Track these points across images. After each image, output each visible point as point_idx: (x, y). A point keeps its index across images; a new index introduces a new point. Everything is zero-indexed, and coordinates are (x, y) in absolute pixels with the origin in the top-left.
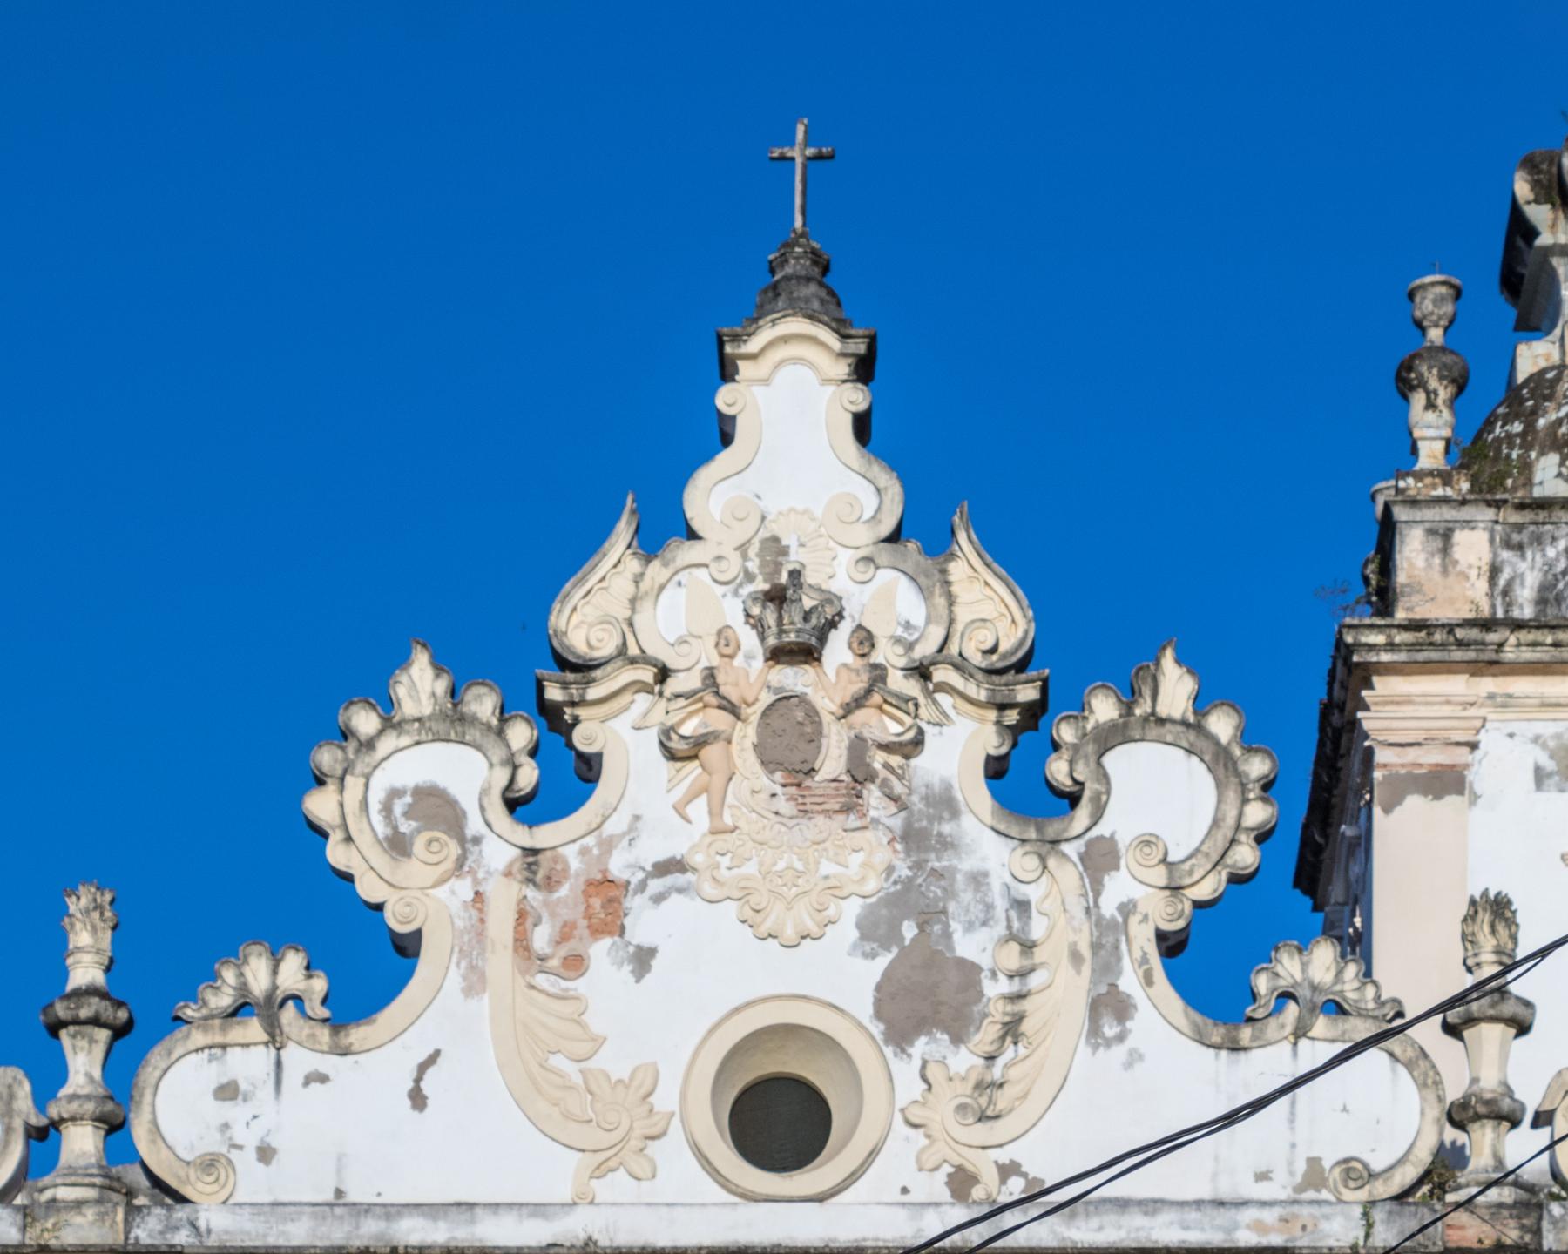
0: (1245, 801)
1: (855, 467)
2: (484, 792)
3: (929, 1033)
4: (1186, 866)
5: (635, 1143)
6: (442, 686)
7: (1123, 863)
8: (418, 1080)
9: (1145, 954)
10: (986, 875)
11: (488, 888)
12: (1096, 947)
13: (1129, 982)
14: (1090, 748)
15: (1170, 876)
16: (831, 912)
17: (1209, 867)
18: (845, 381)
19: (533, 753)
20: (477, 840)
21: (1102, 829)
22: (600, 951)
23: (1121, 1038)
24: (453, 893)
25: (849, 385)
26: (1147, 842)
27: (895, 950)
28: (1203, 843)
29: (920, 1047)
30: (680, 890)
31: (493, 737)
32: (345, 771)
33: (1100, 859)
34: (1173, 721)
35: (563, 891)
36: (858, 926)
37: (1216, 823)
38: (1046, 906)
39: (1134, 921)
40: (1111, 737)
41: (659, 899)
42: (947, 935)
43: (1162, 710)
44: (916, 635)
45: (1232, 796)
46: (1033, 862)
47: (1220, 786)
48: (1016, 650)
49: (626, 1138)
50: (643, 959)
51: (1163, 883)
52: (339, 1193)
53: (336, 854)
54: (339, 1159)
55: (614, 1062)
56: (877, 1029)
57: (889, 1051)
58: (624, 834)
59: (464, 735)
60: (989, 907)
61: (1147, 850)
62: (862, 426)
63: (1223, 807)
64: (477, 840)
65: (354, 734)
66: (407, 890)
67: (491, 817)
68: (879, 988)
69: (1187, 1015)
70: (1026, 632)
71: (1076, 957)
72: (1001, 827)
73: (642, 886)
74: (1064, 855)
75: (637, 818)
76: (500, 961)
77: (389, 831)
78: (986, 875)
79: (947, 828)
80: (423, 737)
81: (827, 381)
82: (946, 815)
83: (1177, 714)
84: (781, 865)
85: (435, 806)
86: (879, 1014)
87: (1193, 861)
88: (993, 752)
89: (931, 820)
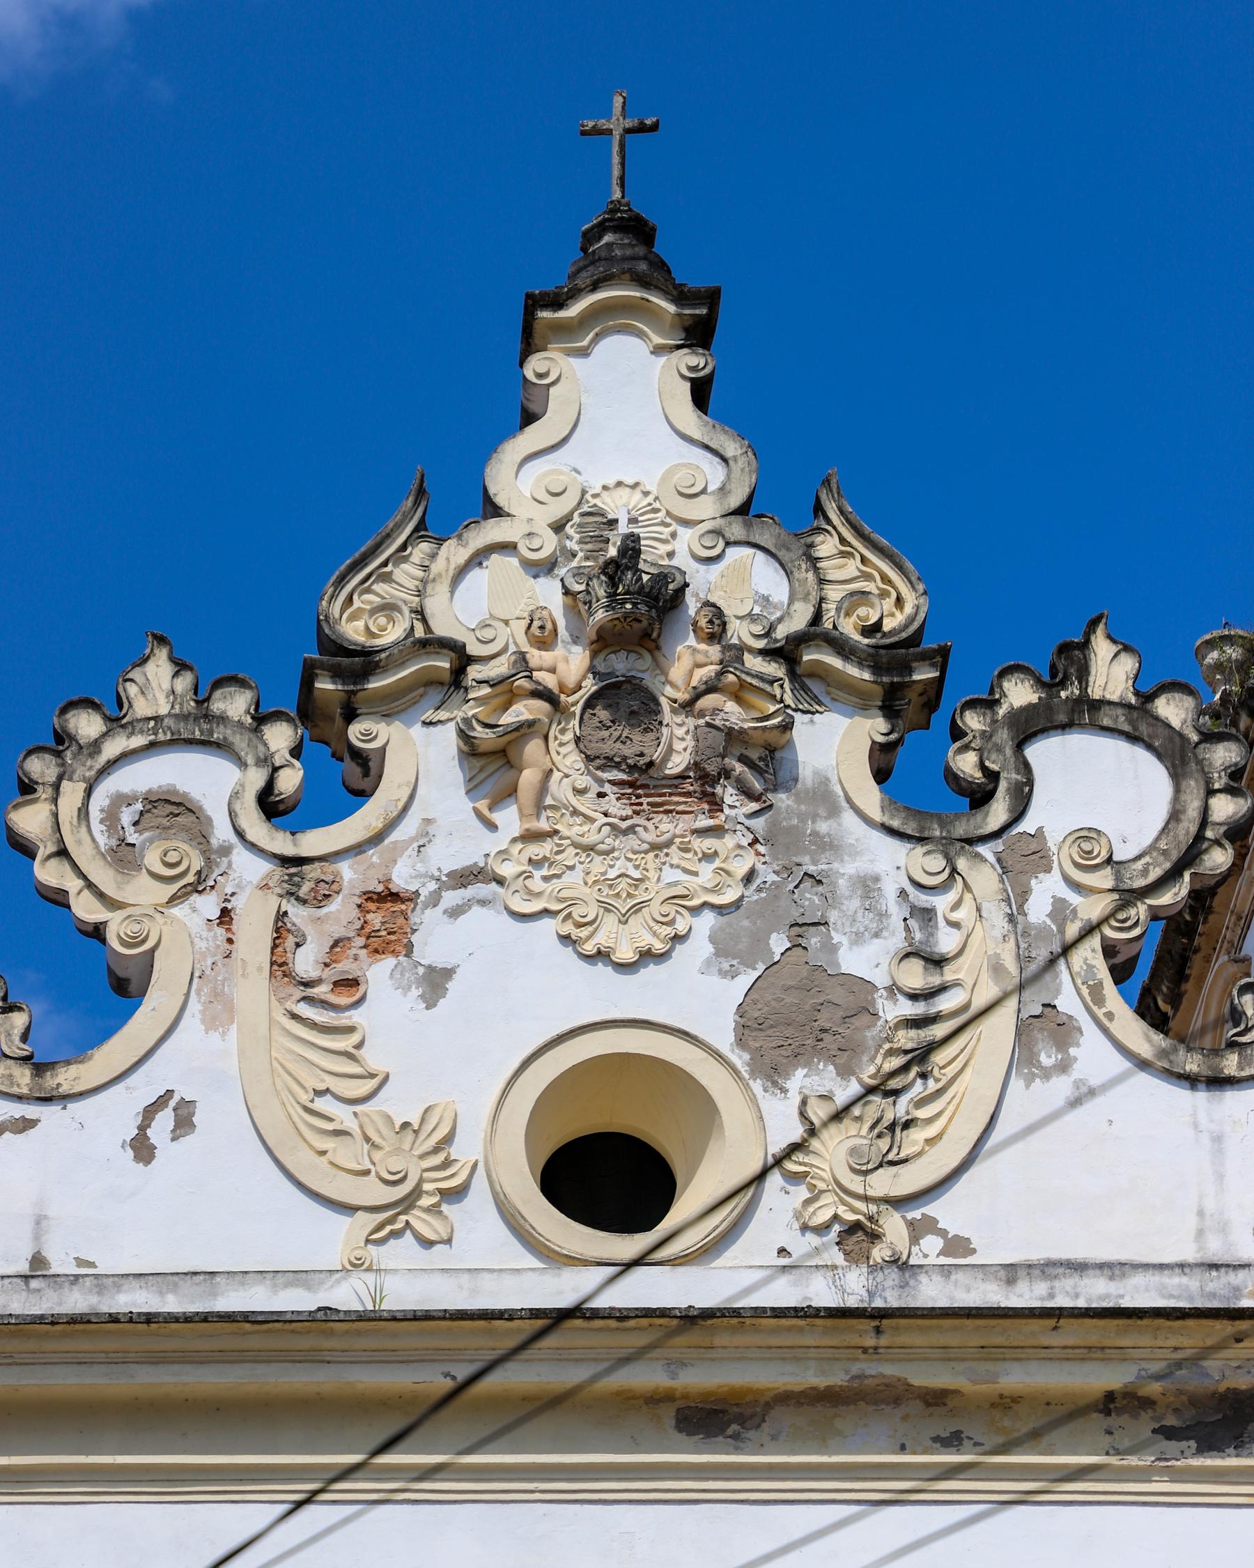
0: (1210, 792)
1: (697, 435)
2: (235, 795)
3: (808, 1064)
4: (1139, 865)
5: (426, 1201)
6: (184, 683)
7: (1055, 865)
8: (143, 1128)
9: (1090, 967)
10: (877, 879)
11: (237, 904)
13: (1068, 1002)
14: (1004, 736)
15: (1118, 877)
16: (681, 927)
17: (1168, 865)
18: (679, 347)
19: (296, 752)
20: (226, 850)
21: (1028, 825)
22: (379, 974)
24: (194, 910)
25: (686, 351)
27: (761, 967)
28: (1157, 839)
29: (798, 1080)
30: (483, 903)
31: (247, 735)
32: (60, 778)
33: (1021, 862)
34: (1110, 703)
35: (334, 906)
36: (712, 939)
37: (1175, 815)
38: (955, 916)
40: (1028, 727)
41: (455, 912)
42: (831, 949)
43: (1095, 692)
44: (778, 614)
45: (1193, 788)
46: (937, 862)
47: (1177, 776)
48: (906, 626)
49: (417, 1192)
50: (436, 982)
51: (1109, 884)
52: (38, 1261)
53: (49, 873)
54: (38, 1223)
55: (399, 1103)
56: (740, 1059)
57: (757, 1086)
58: (412, 840)
59: (211, 732)
60: (883, 915)
61: (1086, 846)
62: (701, 392)
63: (1183, 797)
64: (226, 850)
65: (72, 738)
66: (136, 908)
67: (244, 823)
68: (741, 1010)
69: (1149, 1040)
70: (918, 607)
72: (895, 823)
73: (435, 900)
74: (978, 855)
75: (428, 821)
76: (252, 988)
77: (114, 842)
78: (877, 879)
79: (823, 827)
80: (161, 737)
81: (658, 350)
82: (822, 812)
83: (1115, 697)
84: (612, 874)
85: (170, 809)
86: (740, 1042)
87: (1147, 859)
88: (880, 739)
89: (803, 818)
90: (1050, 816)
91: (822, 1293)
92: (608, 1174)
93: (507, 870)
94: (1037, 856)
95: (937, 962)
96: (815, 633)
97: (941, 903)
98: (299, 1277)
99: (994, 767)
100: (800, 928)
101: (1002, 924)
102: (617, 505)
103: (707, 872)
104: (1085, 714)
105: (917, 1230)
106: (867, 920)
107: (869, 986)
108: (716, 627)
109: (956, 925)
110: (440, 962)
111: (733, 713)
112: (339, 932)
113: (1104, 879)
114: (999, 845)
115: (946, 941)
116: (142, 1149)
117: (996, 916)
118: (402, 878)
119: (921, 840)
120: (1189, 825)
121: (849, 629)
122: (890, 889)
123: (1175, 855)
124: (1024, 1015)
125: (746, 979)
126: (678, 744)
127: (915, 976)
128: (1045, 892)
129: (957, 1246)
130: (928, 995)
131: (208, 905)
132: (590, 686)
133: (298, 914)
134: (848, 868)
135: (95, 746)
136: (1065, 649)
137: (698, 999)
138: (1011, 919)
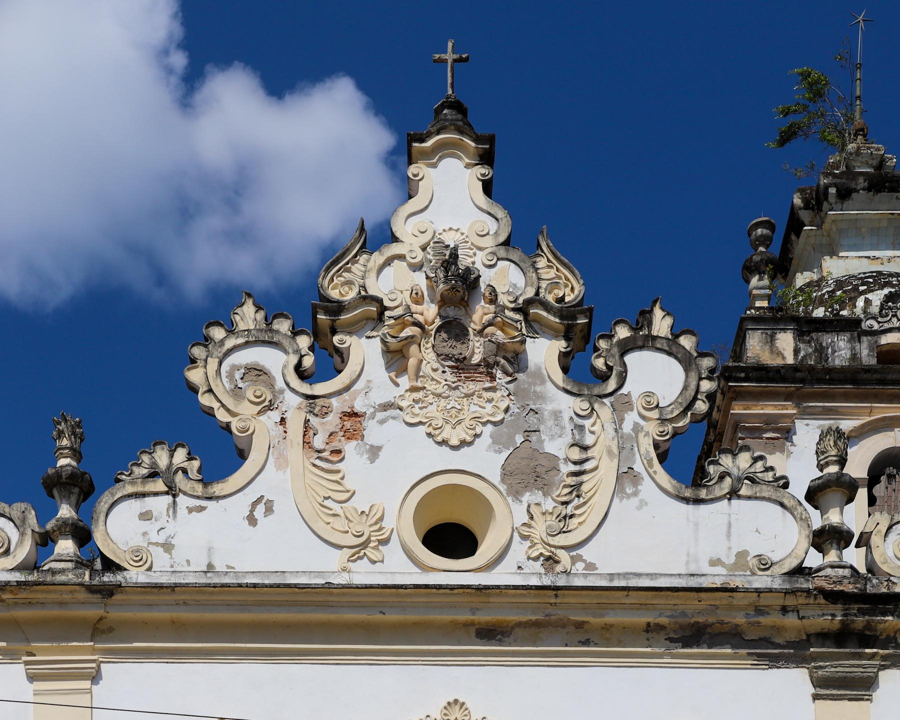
0: (701, 379)
4: (670, 409)
9: (648, 452)
12: (621, 449)
14: (615, 350)
15: (661, 414)
17: (682, 409)
21: (624, 391)
26: (649, 394)
37: (685, 388)
38: (593, 429)
39: (641, 435)
46: (586, 405)
51: (657, 416)
63: (689, 380)
71: (610, 452)
74: (603, 402)
94: (628, 404)
95: (585, 448)
97: (587, 423)
99: (611, 364)
101: (613, 433)
104: (648, 342)
109: (593, 433)
113: (655, 414)
114: (612, 399)
115: (589, 440)
117: (610, 428)
119: (578, 395)
120: (691, 392)
123: (685, 405)
124: (620, 472)
128: (631, 418)
138: (616, 430)
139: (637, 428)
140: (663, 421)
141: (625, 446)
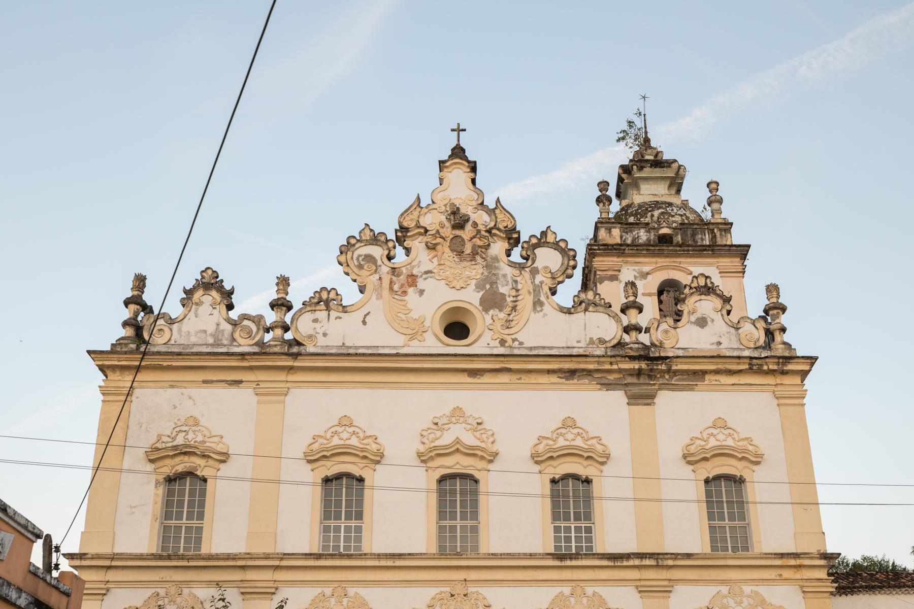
2: (382, 255)
12: (534, 291)
13: (543, 298)
22: (411, 290)
23: (541, 311)
26: (546, 268)
29: (491, 312)
33: (534, 272)
37: (562, 264)
41: (425, 279)
42: (497, 288)
45: (566, 259)
50: (421, 292)
55: (414, 315)
56: (481, 308)
71: (529, 292)
73: (421, 276)
76: (386, 292)
85: (369, 258)
86: (481, 305)
90: (539, 264)
91: (495, 352)
92: (457, 329)
93: (435, 271)
95: (517, 290)
96: (495, 227)
98: (395, 347)
100: (492, 284)
102: (457, 203)
103: (474, 271)
105: (514, 340)
106: (505, 282)
107: (505, 295)
108: (475, 224)
110: (422, 288)
111: (478, 242)
112: (402, 282)
115: (520, 287)
116: (364, 323)
117: (529, 282)
118: (415, 272)
121: (501, 227)
122: (509, 276)
125: (482, 293)
126: (468, 249)
127: (514, 293)
128: (539, 278)
129: (521, 343)
130: (516, 296)
131: (377, 276)
132: (452, 236)
133: (394, 278)
134: (501, 272)
135: (354, 245)
136: (542, 232)
137: (471, 297)
139: (541, 282)
140: (553, 278)
141: (537, 289)
